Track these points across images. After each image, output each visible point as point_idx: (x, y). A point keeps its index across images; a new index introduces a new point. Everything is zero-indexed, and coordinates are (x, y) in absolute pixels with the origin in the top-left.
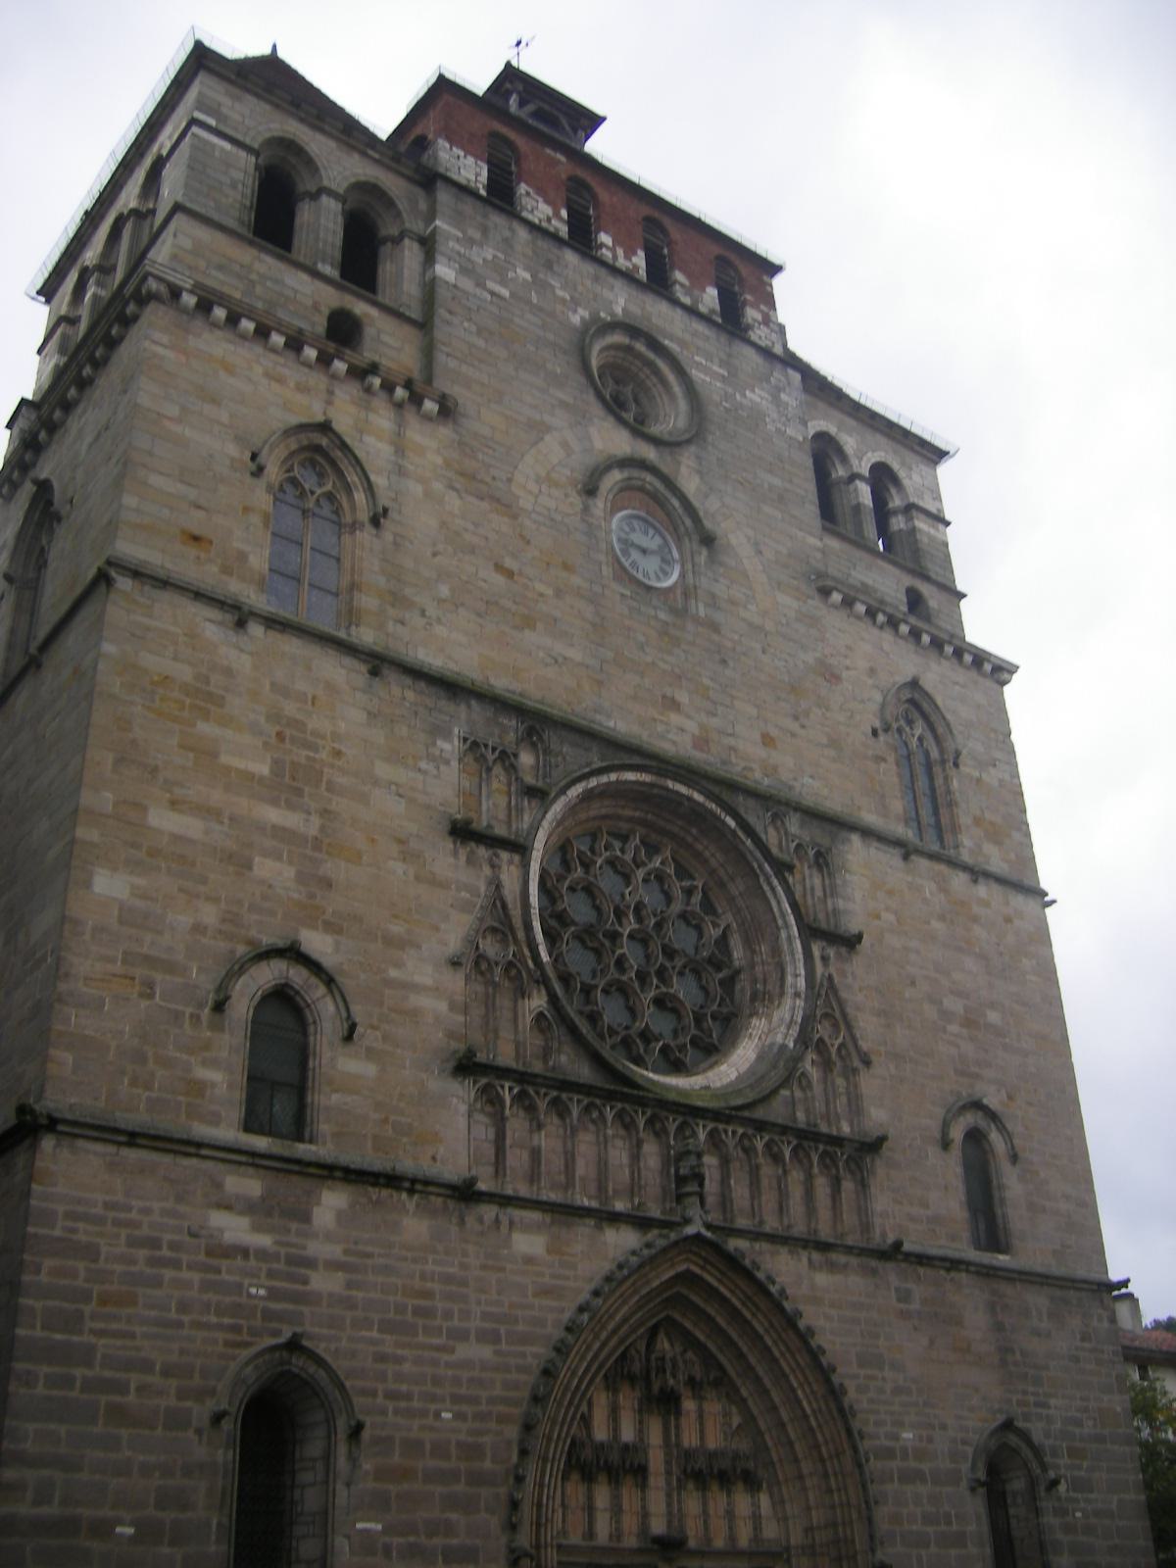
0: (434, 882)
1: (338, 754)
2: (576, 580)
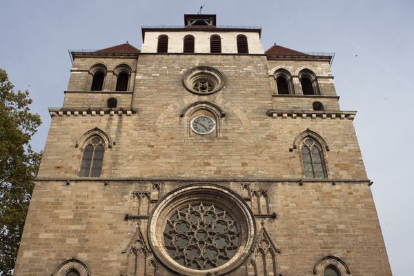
0: (119, 233)
1: (93, 207)
2: (175, 141)
